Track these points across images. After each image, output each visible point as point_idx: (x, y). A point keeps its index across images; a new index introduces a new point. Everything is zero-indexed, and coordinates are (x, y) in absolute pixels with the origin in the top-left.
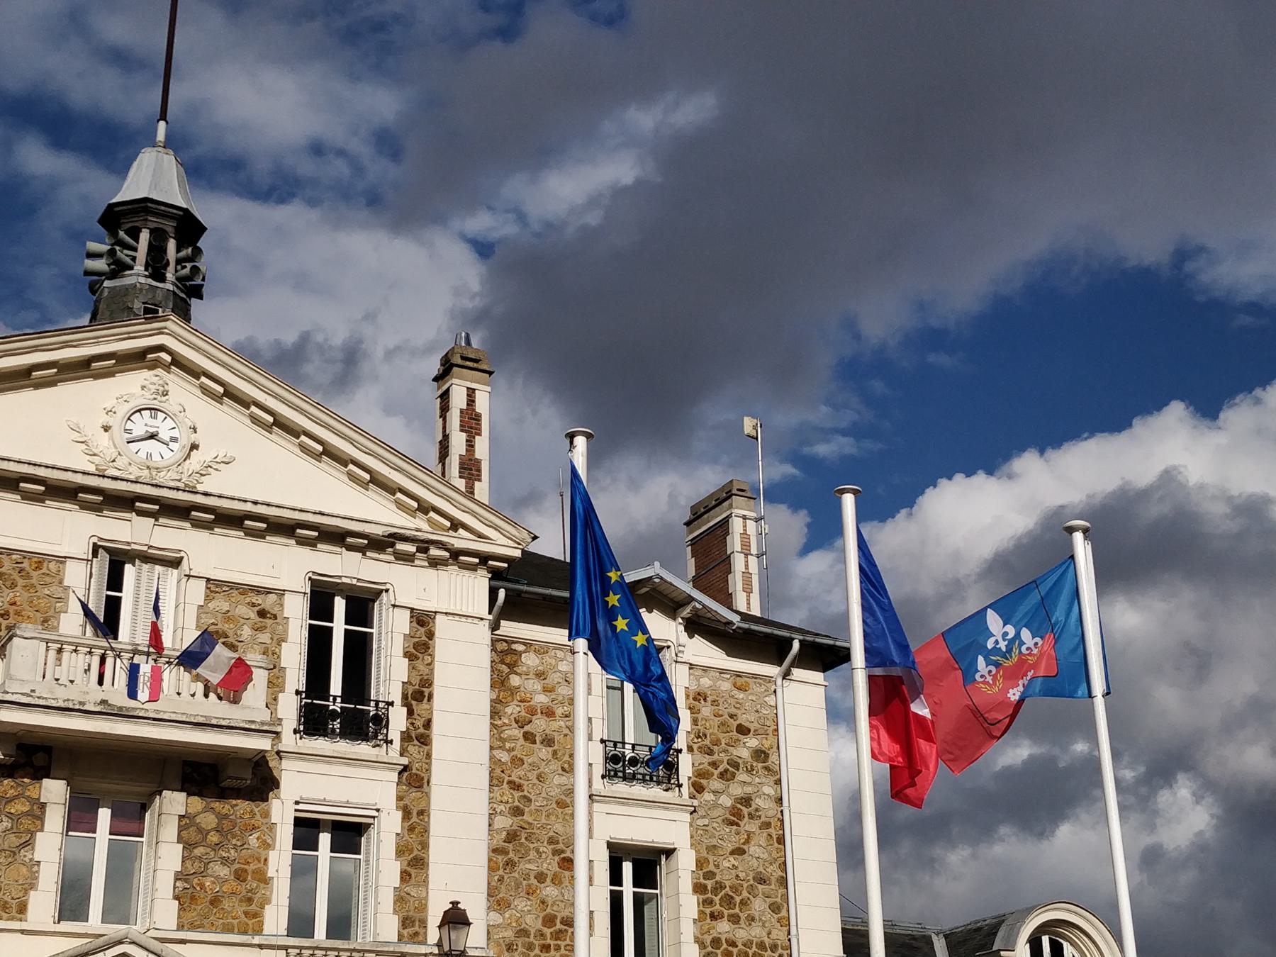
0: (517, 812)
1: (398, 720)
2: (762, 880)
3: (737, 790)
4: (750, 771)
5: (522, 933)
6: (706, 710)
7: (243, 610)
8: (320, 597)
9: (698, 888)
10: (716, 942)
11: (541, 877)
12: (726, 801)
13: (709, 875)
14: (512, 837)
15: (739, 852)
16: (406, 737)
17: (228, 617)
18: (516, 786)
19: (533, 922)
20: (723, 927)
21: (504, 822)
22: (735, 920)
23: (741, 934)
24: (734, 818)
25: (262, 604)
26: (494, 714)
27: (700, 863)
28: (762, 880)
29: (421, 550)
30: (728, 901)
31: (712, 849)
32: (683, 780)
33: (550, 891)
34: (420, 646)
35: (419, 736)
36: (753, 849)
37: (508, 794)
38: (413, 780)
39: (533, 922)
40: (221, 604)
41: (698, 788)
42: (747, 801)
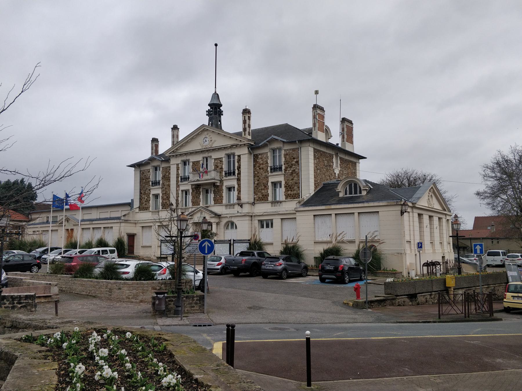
0: (258, 180)
1: (237, 172)
2: (296, 183)
3: (292, 169)
4: (295, 165)
5: (259, 198)
6: (288, 157)
7: (219, 162)
8: (229, 156)
9: (285, 187)
10: (288, 195)
11: (262, 189)
12: (291, 171)
13: (287, 184)
14: (258, 184)
15: (293, 179)
16: (238, 174)
17: (217, 163)
18: (258, 177)
19: (261, 196)
20: (289, 192)
21: (256, 182)
22: (291, 191)
23: (292, 193)
24: (292, 173)
25: (220, 160)
26: (254, 166)
27: (286, 183)
28: (296, 183)
29: (236, 146)
30: (290, 188)
31: (288, 180)
32: (283, 170)
33: (263, 191)
34: (239, 161)
35: (239, 174)
36: (295, 179)
37: (256, 178)
38: (239, 180)
39: (261, 196)
40: (216, 161)
41: (285, 170)
42: (294, 170)
